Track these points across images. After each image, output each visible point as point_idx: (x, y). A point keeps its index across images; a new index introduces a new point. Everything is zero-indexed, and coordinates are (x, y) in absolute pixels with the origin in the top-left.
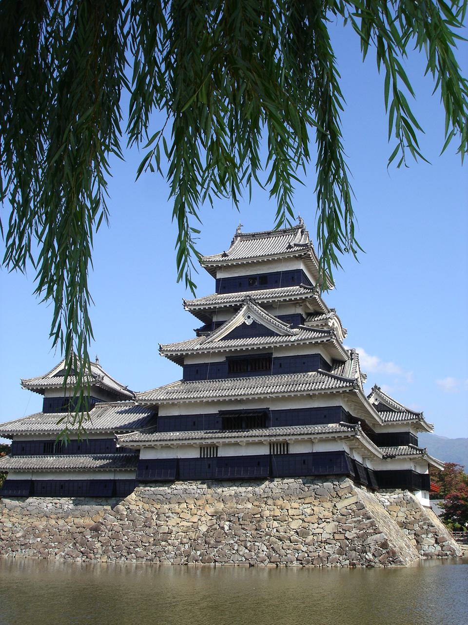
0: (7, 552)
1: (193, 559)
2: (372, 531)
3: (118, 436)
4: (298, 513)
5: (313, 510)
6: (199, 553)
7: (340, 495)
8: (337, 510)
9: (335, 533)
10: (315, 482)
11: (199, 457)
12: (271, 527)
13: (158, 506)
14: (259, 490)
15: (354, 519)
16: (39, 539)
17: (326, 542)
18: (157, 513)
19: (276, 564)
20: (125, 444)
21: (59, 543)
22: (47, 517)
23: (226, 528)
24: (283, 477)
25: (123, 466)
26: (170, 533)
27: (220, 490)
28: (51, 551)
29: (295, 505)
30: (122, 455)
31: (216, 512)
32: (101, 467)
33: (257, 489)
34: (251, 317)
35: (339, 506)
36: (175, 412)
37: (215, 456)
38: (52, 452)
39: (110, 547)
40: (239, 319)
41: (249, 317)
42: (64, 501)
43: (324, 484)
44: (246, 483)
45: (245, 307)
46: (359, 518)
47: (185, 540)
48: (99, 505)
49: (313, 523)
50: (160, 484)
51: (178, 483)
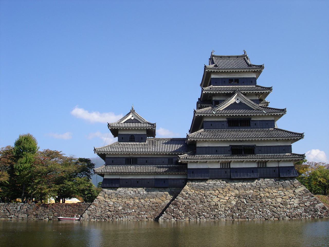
0: (117, 218)
1: (236, 218)
2: (316, 202)
3: (179, 156)
4: (278, 195)
5: (284, 193)
6: (237, 214)
7: (296, 187)
8: (296, 193)
9: (299, 203)
10: (281, 180)
11: (220, 168)
12: (268, 201)
13: (204, 192)
14: (254, 183)
15: (306, 197)
16: (133, 210)
17: (297, 207)
18: (204, 196)
19: (278, 218)
20: (183, 160)
21: (146, 212)
22: (133, 198)
23: (245, 202)
24: (264, 178)
25: (177, 171)
26: (218, 205)
27: (233, 184)
28: (143, 216)
29: (275, 191)
30: (168, 166)
31: (236, 195)
32: (165, 172)
33: (252, 184)
34: (239, 100)
35: (297, 191)
36: (206, 145)
37: (228, 167)
38: (130, 163)
39: (188, 213)
40: (233, 100)
41: (238, 99)
42: (140, 190)
43: (286, 181)
44: (246, 180)
45: (236, 94)
46: (308, 197)
47: (227, 209)
48: (160, 192)
49: (287, 199)
50: (200, 181)
51: (209, 180)
